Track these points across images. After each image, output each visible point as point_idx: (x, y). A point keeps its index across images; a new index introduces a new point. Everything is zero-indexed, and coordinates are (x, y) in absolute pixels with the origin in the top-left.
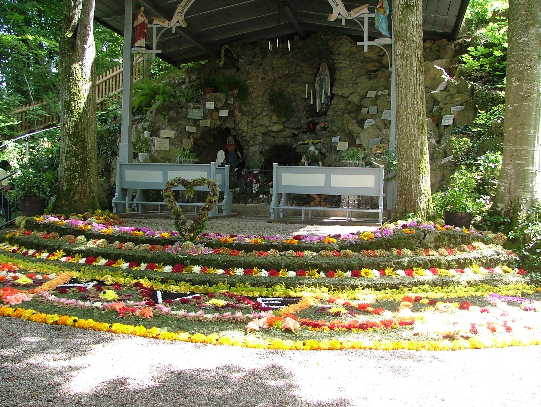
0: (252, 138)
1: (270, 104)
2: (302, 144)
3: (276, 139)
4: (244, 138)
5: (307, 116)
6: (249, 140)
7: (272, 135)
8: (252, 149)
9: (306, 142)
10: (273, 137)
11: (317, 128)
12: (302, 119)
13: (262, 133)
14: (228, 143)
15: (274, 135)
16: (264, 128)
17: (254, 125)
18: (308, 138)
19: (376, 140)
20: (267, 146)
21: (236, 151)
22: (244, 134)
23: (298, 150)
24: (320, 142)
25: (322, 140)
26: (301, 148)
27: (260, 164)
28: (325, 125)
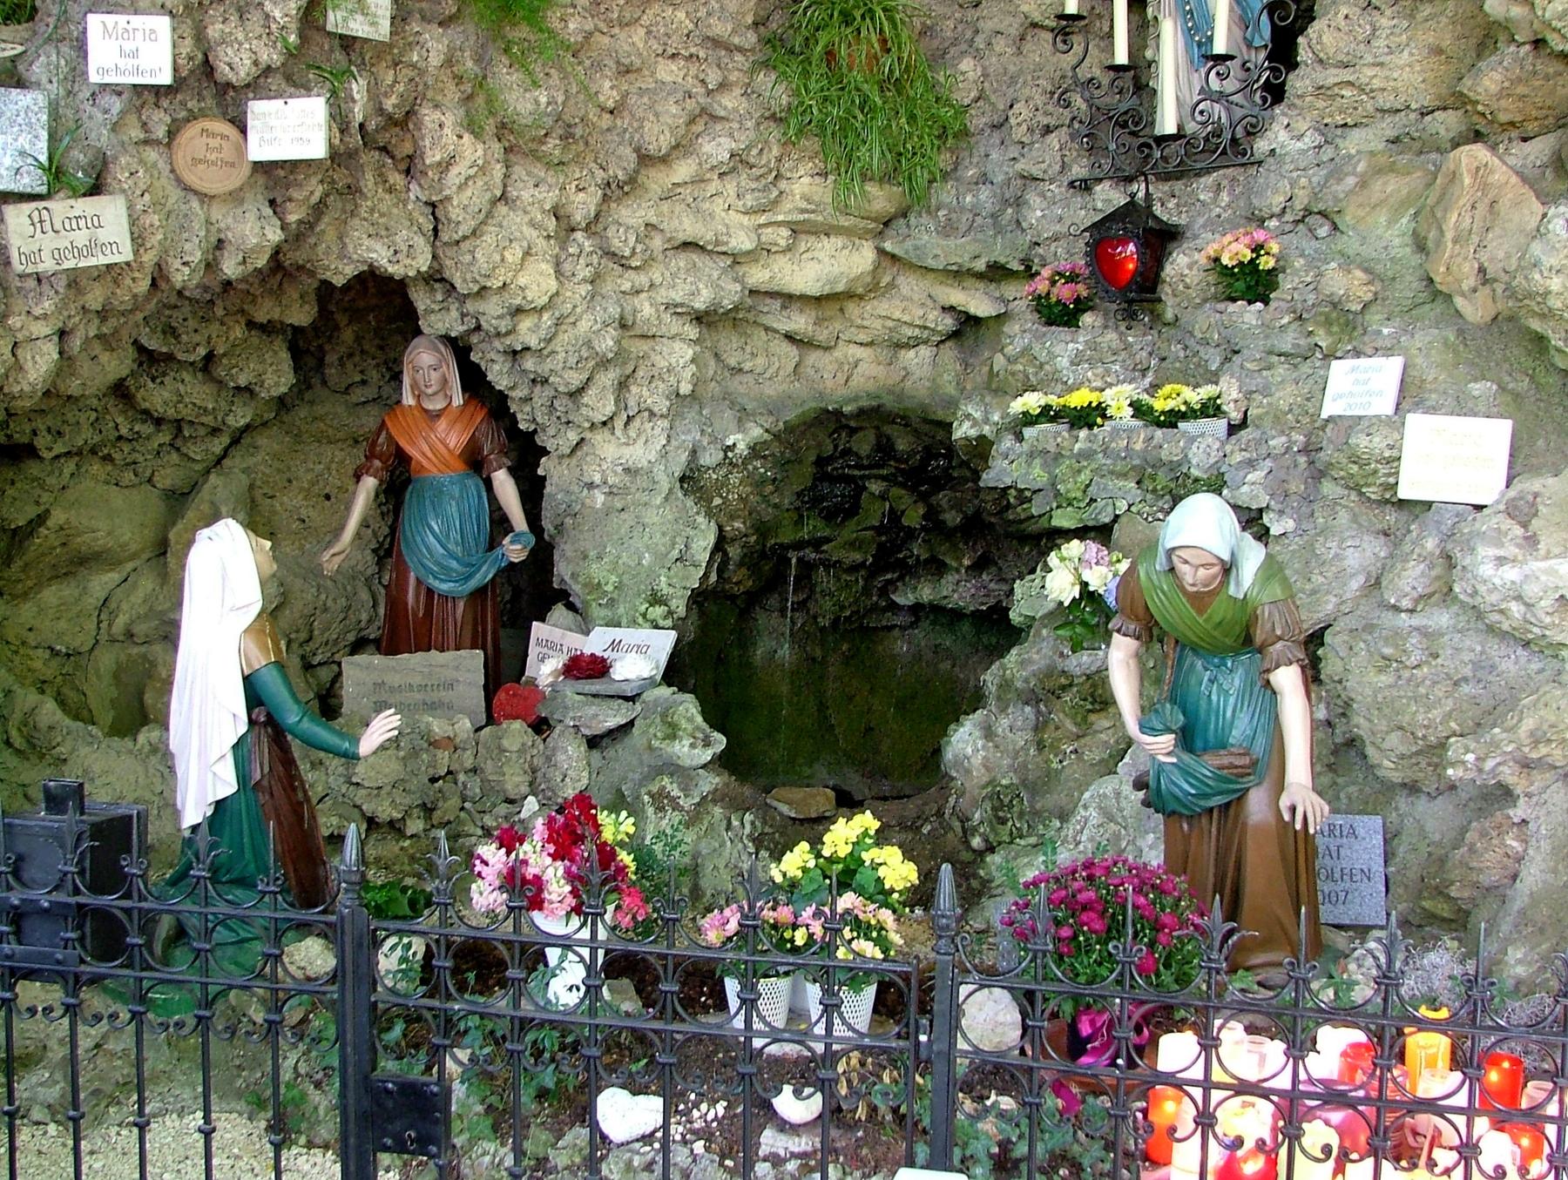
0: (604, 363)
1: (766, 65)
2: (1047, 414)
3: (814, 357)
4: (529, 363)
5: (1079, 171)
6: (575, 379)
7: (784, 326)
8: (611, 452)
9: (1079, 399)
10: (789, 337)
11: (1169, 271)
12: (1033, 199)
13: (700, 318)
14: (408, 399)
15: (799, 322)
16: (712, 268)
17: (621, 241)
18: (1093, 356)
20: (743, 416)
21: (475, 462)
22: (528, 332)
23: (1004, 470)
24: (1211, 409)
25: (1229, 391)
26: (1031, 455)
27: (679, 586)
28: (1257, 249)
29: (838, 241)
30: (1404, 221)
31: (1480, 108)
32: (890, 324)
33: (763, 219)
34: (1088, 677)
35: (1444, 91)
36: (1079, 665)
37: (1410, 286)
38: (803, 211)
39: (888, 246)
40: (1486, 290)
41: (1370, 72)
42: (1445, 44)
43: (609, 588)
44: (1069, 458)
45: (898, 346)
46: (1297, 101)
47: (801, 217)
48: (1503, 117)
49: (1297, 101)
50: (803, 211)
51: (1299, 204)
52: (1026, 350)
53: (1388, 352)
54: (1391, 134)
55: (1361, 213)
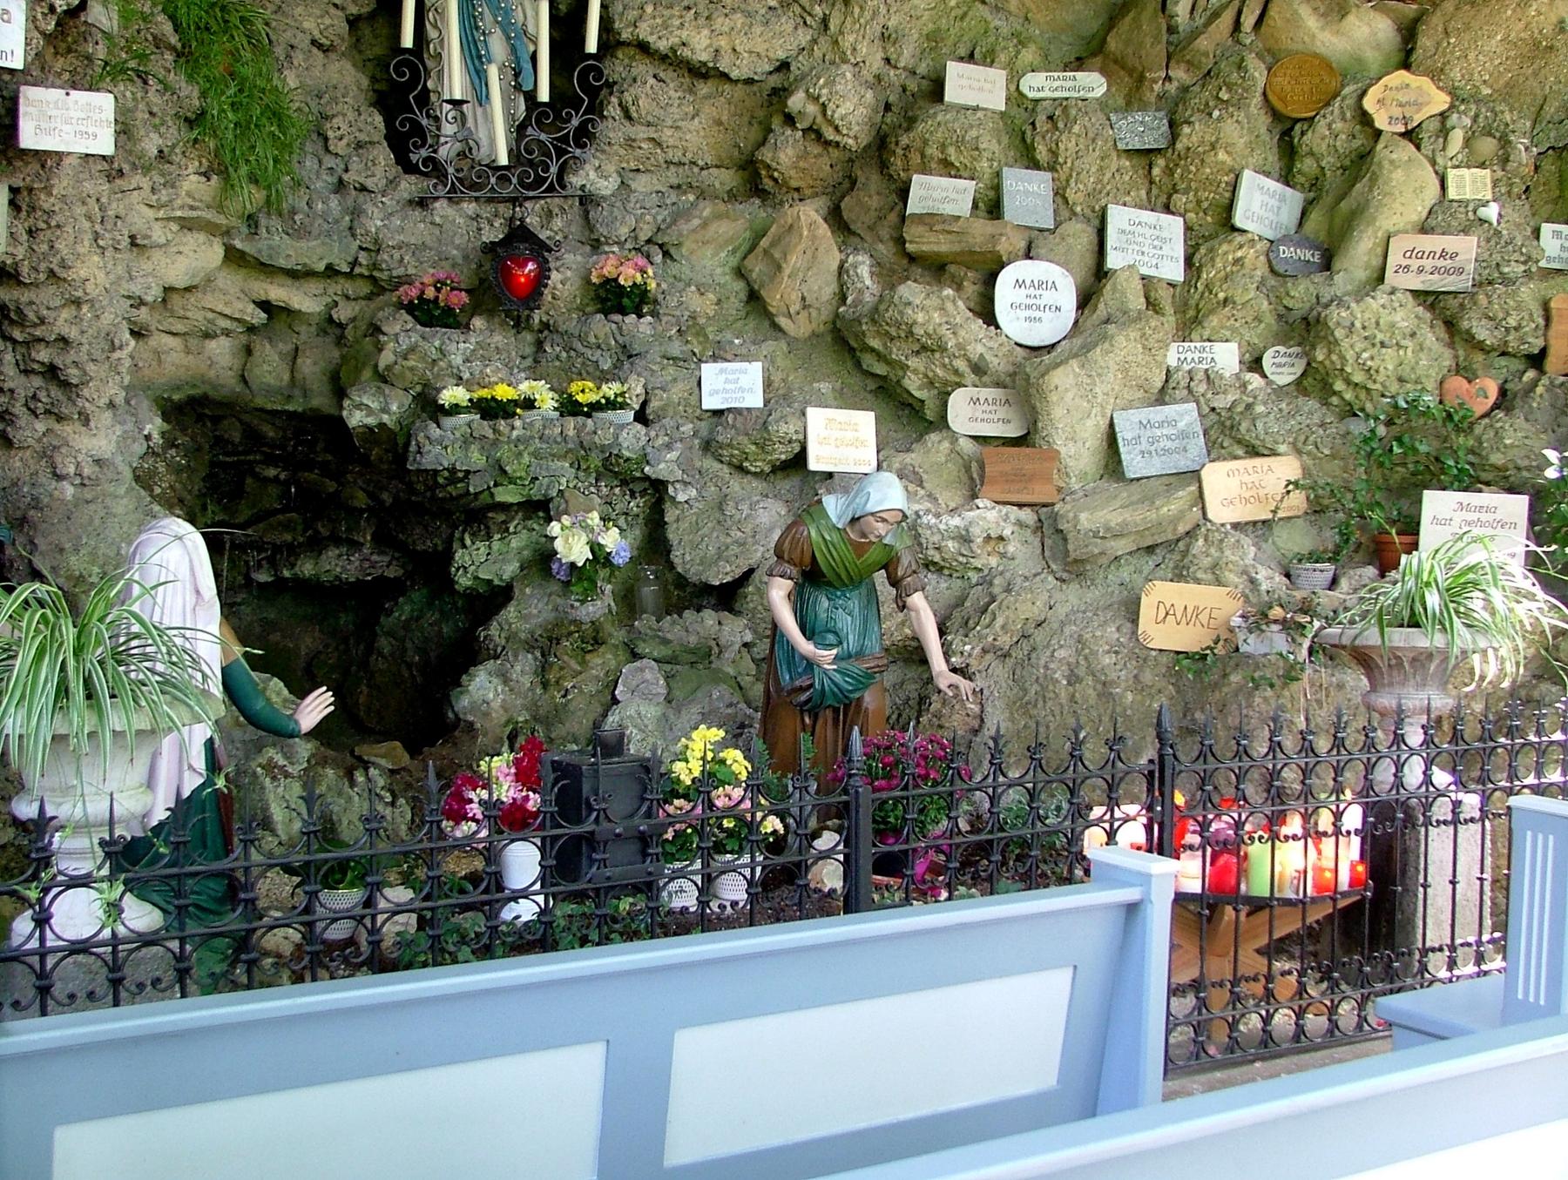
9: (503, 392)
12: (369, 208)
18: (483, 354)
19: (1172, 423)
22: (62, 322)
25: (635, 388)
29: (201, 237)
30: (723, 255)
31: (776, 174)
32: (210, 315)
33: (161, 214)
34: (593, 622)
35: (724, 155)
36: (588, 614)
37: (735, 304)
38: (192, 208)
39: (238, 244)
40: (804, 314)
41: (669, 132)
42: (724, 118)
43: (94, 579)
44: (508, 443)
45: (207, 336)
46: (607, 148)
47: (194, 214)
48: (794, 184)
49: (607, 148)
50: (192, 208)
51: (643, 237)
52: (412, 349)
53: (747, 358)
54: (675, 181)
55: (694, 246)
